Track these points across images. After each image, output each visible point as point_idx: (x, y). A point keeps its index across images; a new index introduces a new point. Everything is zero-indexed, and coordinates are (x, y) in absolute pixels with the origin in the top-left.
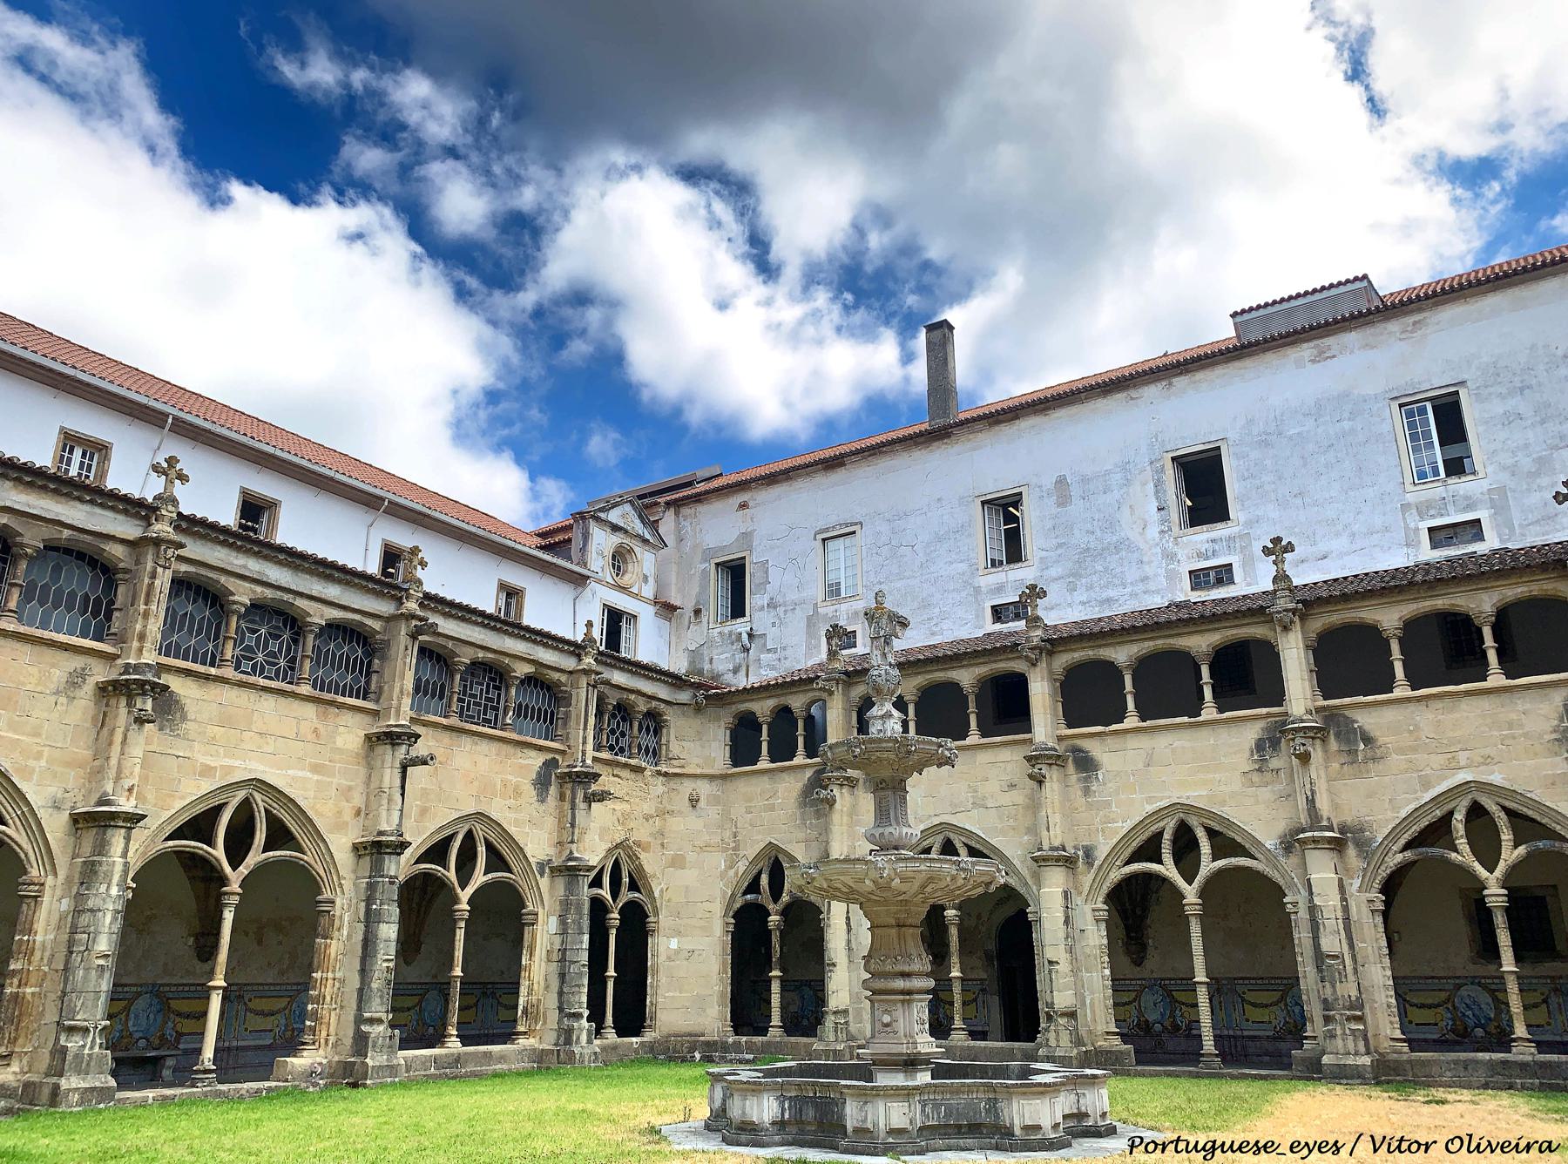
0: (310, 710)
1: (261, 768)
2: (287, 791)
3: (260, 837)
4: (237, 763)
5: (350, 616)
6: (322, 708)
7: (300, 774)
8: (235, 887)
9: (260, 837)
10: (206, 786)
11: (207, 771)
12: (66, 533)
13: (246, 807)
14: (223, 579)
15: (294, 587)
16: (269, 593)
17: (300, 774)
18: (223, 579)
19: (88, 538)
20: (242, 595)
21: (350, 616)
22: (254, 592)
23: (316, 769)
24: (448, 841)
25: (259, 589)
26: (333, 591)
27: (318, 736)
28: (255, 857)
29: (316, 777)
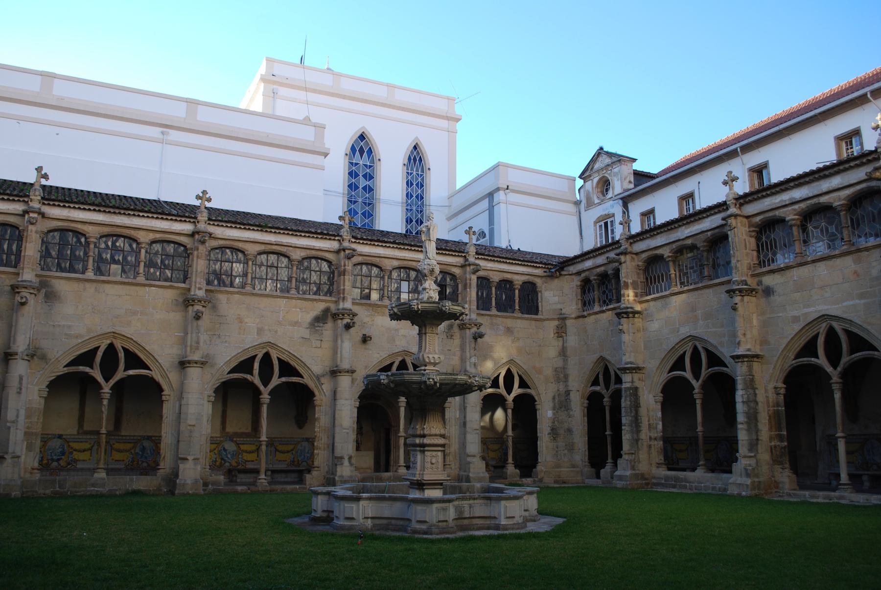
0: (848, 261)
1: (826, 307)
2: (844, 316)
3: (845, 347)
4: (812, 309)
5: (858, 187)
6: (855, 256)
7: (851, 303)
8: (835, 378)
9: (845, 347)
10: (797, 327)
11: (796, 319)
12: (709, 233)
13: (831, 332)
14: (777, 213)
15: (811, 195)
16: (803, 205)
17: (851, 303)
18: (777, 213)
19: (717, 231)
20: (790, 214)
21: (858, 187)
22: (795, 210)
23: (861, 296)
24: (682, 358)
25: (796, 207)
26: (836, 181)
27: (858, 275)
28: (845, 359)
29: (863, 301)
